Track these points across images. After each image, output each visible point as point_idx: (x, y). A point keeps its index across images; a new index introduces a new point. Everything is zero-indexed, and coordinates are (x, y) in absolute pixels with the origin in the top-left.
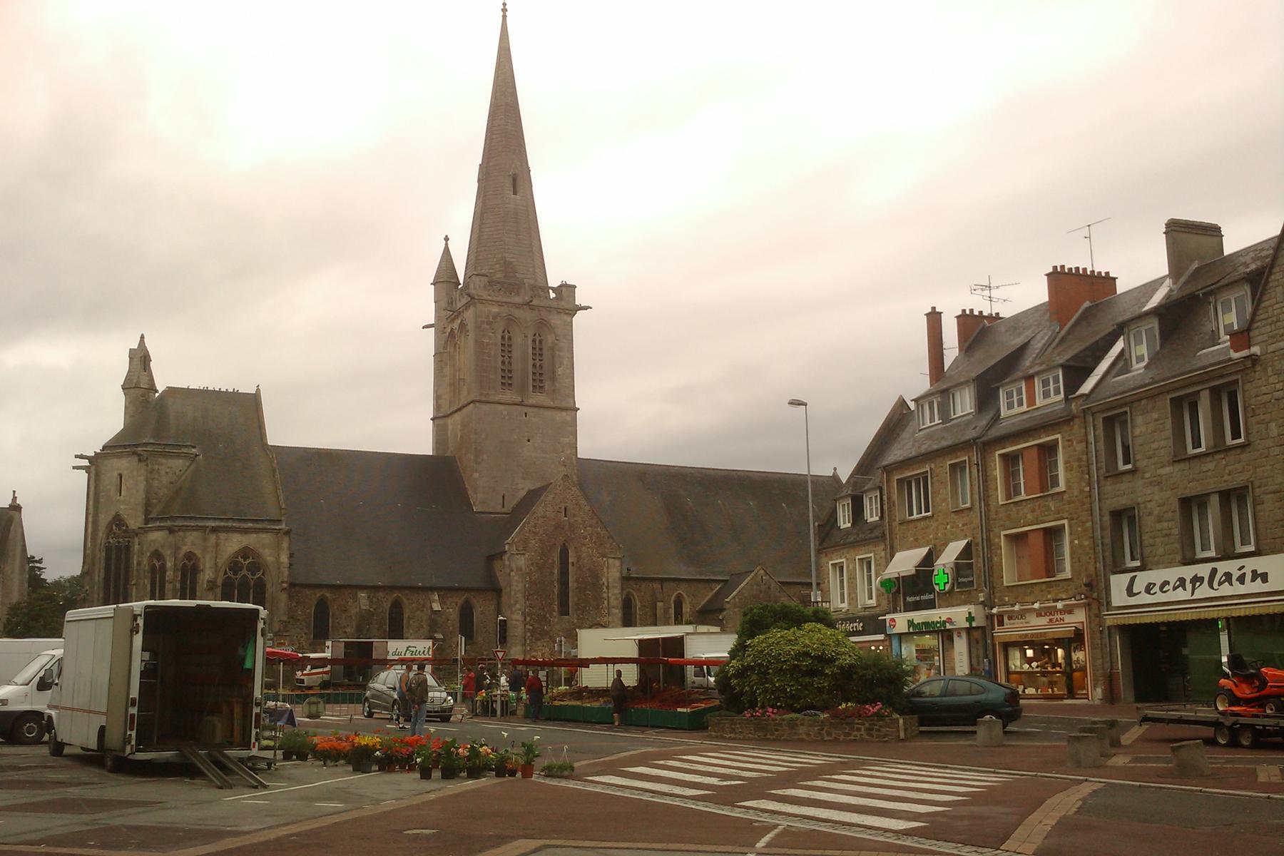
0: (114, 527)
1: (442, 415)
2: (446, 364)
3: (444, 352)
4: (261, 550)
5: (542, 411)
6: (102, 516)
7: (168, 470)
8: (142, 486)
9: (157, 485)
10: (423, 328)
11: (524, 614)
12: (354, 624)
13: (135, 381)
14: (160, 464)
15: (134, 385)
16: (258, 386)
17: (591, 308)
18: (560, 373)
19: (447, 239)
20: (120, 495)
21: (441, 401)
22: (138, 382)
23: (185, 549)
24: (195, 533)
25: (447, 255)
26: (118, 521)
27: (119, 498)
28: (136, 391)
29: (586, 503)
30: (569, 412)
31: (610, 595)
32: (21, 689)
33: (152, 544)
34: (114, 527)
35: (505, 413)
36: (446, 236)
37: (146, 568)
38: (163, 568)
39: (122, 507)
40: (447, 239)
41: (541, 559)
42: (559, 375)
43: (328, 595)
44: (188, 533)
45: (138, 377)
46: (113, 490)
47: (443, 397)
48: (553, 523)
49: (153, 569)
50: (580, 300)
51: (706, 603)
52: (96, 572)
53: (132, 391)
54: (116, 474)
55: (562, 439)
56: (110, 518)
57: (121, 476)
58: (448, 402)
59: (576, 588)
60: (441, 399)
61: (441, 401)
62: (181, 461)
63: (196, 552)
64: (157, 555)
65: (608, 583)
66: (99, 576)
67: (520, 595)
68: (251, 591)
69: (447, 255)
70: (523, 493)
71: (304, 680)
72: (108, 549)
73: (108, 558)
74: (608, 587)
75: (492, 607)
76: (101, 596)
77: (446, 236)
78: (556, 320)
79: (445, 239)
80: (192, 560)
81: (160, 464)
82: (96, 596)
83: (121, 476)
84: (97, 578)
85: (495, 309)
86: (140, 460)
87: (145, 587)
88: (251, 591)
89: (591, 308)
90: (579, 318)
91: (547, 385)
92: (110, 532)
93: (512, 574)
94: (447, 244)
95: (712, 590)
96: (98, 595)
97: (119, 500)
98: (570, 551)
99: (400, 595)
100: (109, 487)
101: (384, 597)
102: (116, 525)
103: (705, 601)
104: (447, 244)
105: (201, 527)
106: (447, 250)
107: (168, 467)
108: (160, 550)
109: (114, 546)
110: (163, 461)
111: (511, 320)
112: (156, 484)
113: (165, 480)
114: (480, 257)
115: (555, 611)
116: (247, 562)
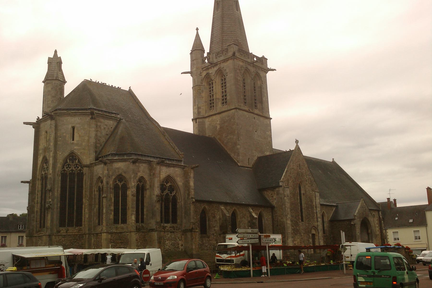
0: (68, 161)
1: (200, 117)
2: (203, 91)
3: (202, 85)
4: (176, 178)
5: (260, 117)
6: (59, 153)
7: (105, 126)
8: (93, 134)
9: (99, 135)
10: (182, 73)
11: (292, 221)
12: (218, 225)
13: (55, 76)
14: (101, 122)
15: (55, 78)
16: (130, 87)
17: (276, 70)
18: (264, 100)
19: (197, 29)
20: (73, 140)
21: (201, 110)
22: (57, 77)
23: (140, 174)
24: (144, 165)
25: (198, 39)
26: (72, 156)
27: (73, 142)
28: (57, 82)
29: (306, 163)
30: (268, 119)
31: (317, 211)
32: (180, 272)
33: (117, 171)
34: (68, 161)
35: (247, 116)
36: (197, 28)
37: (112, 186)
38: (125, 188)
39: (75, 147)
40: (197, 29)
41: (293, 191)
42: (264, 101)
43: (207, 207)
44: (141, 165)
45: (57, 74)
46: (68, 137)
47: (202, 108)
48: (296, 172)
49: (116, 187)
50: (270, 65)
51: (332, 216)
52: (56, 189)
53: (54, 82)
54: (70, 126)
55: (267, 133)
56: (66, 154)
57: (73, 128)
58: (205, 111)
59: (306, 207)
60: (201, 109)
61: (201, 110)
62: (111, 122)
63: (145, 177)
64: (120, 178)
65: (316, 205)
66: (58, 192)
67: (289, 210)
68: (170, 204)
69: (198, 39)
70: (255, 158)
71: (233, 260)
72: (64, 175)
73: (63, 181)
74: (316, 207)
75: (270, 217)
76: (59, 205)
77: (197, 28)
78: (262, 74)
79: (196, 29)
80: (141, 182)
81: (101, 122)
82: (56, 206)
83: (73, 128)
84: (56, 194)
85: (241, 64)
86: (92, 118)
87: (111, 199)
88: (170, 204)
89: (276, 70)
90: (269, 75)
91: (259, 105)
92: (65, 164)
93: (286, 198)
94: (197, 32)
95: (333, 210)
96: (57, 205)
97: (73, 143)
98: (302, 187)
99: (236, 208)
100: (64, 134)
101: (230, 209)
102: (70, 160)
103: (331, 215)
104: (197, 32)
105: (148, 161)
106: (197, 36)
107: (105, 125)
108: (124, 174)
109: (76, 173)
110: (102, 120)
111: (247, 70)
112: (99, 134)
113: (104, 132)
114: (224, 38)
115: (300, 219)
116: (168, 185)
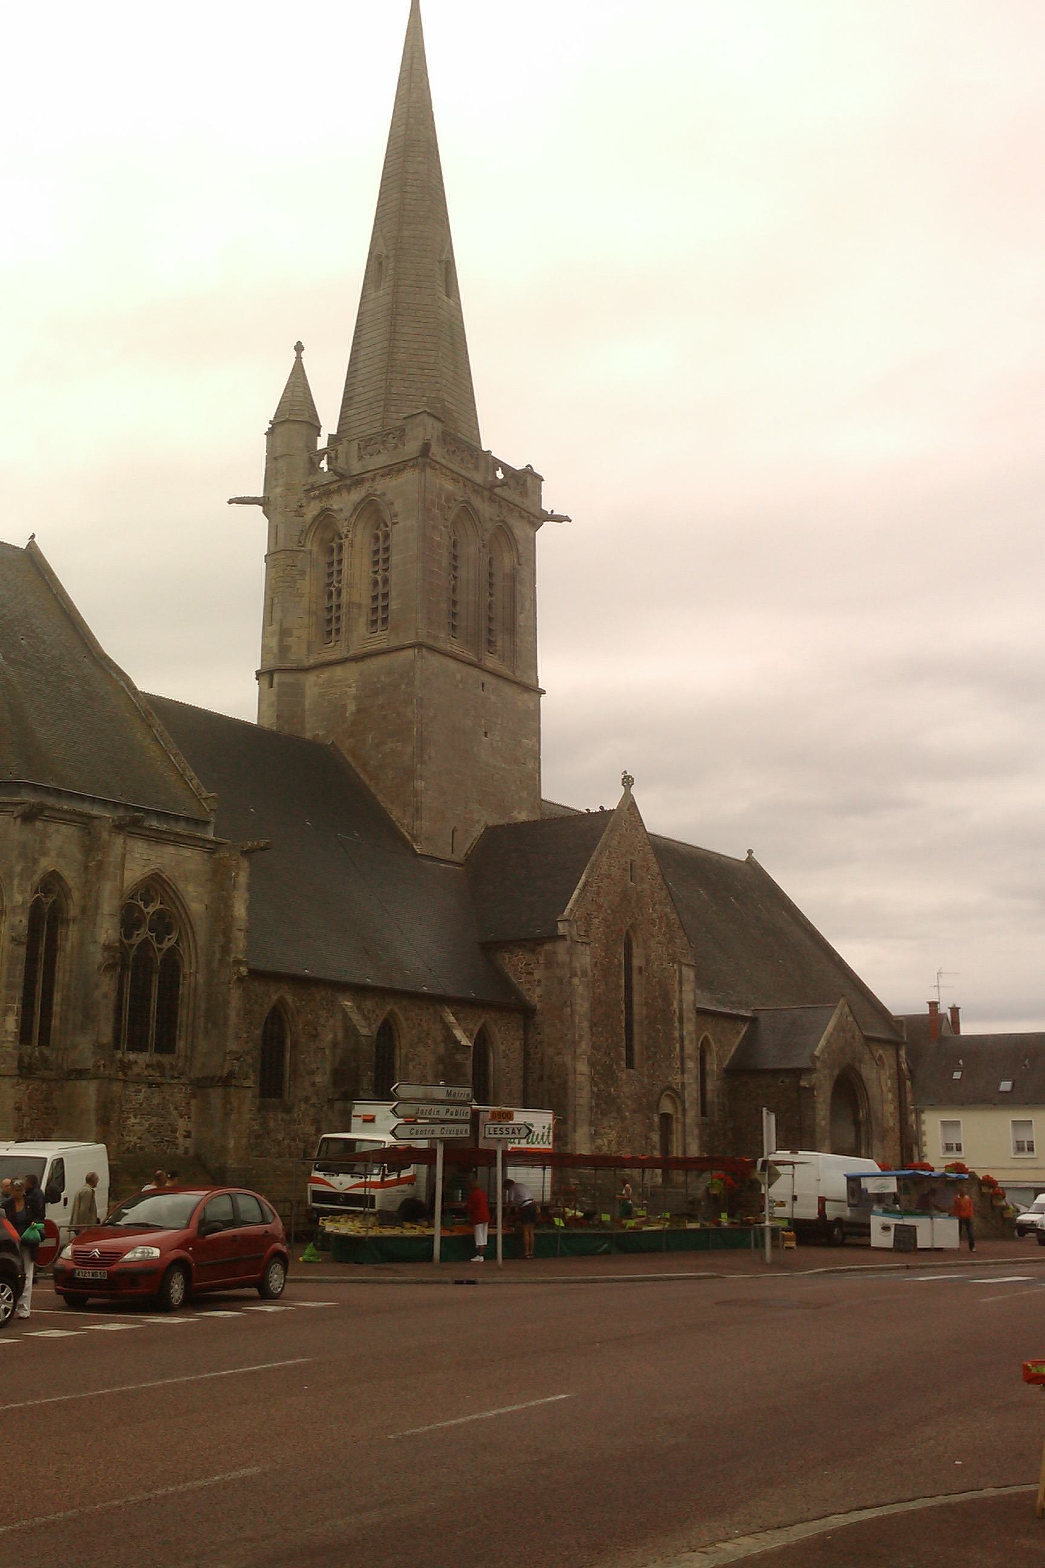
2: (303, 573)
3: (301, 551)
4: (181, 886)
10: (231, 502)
11: (592, 1064)
12: (328, 1068)
17: (570, 521)
19: (299, 348)
21: (288, 641)
23: (46, 864)
24: (65, 829)
25: (298, 381)
30: (533, 693)
35: (458, 677)
36: (299, 343)
40: (299, 348)
42: (520, 626)
43: (289, 999)
44: (52, 827)
47: (296, 633)
51: (733, 1057)
59: (647, 1017)
61: (288, 641)
65: (681, 1009)
67: (585, 1024)
68: (155, 979)
69: (298, 381)
70: (478, 830)
75: (517, 1044)
77: (299, 343)
78: (519, 528)
85: (449, 486)
88: (155, 979)
89: (570, 521)
90: (545, 533)
91: (501, 640)
94: (299, 359)
95: (739, 1033)
98: (634, 945)
99: (396, 1010)
104: (299, 359)
106: (298, 374)
111: (468, 512)
116: (151, 910)
